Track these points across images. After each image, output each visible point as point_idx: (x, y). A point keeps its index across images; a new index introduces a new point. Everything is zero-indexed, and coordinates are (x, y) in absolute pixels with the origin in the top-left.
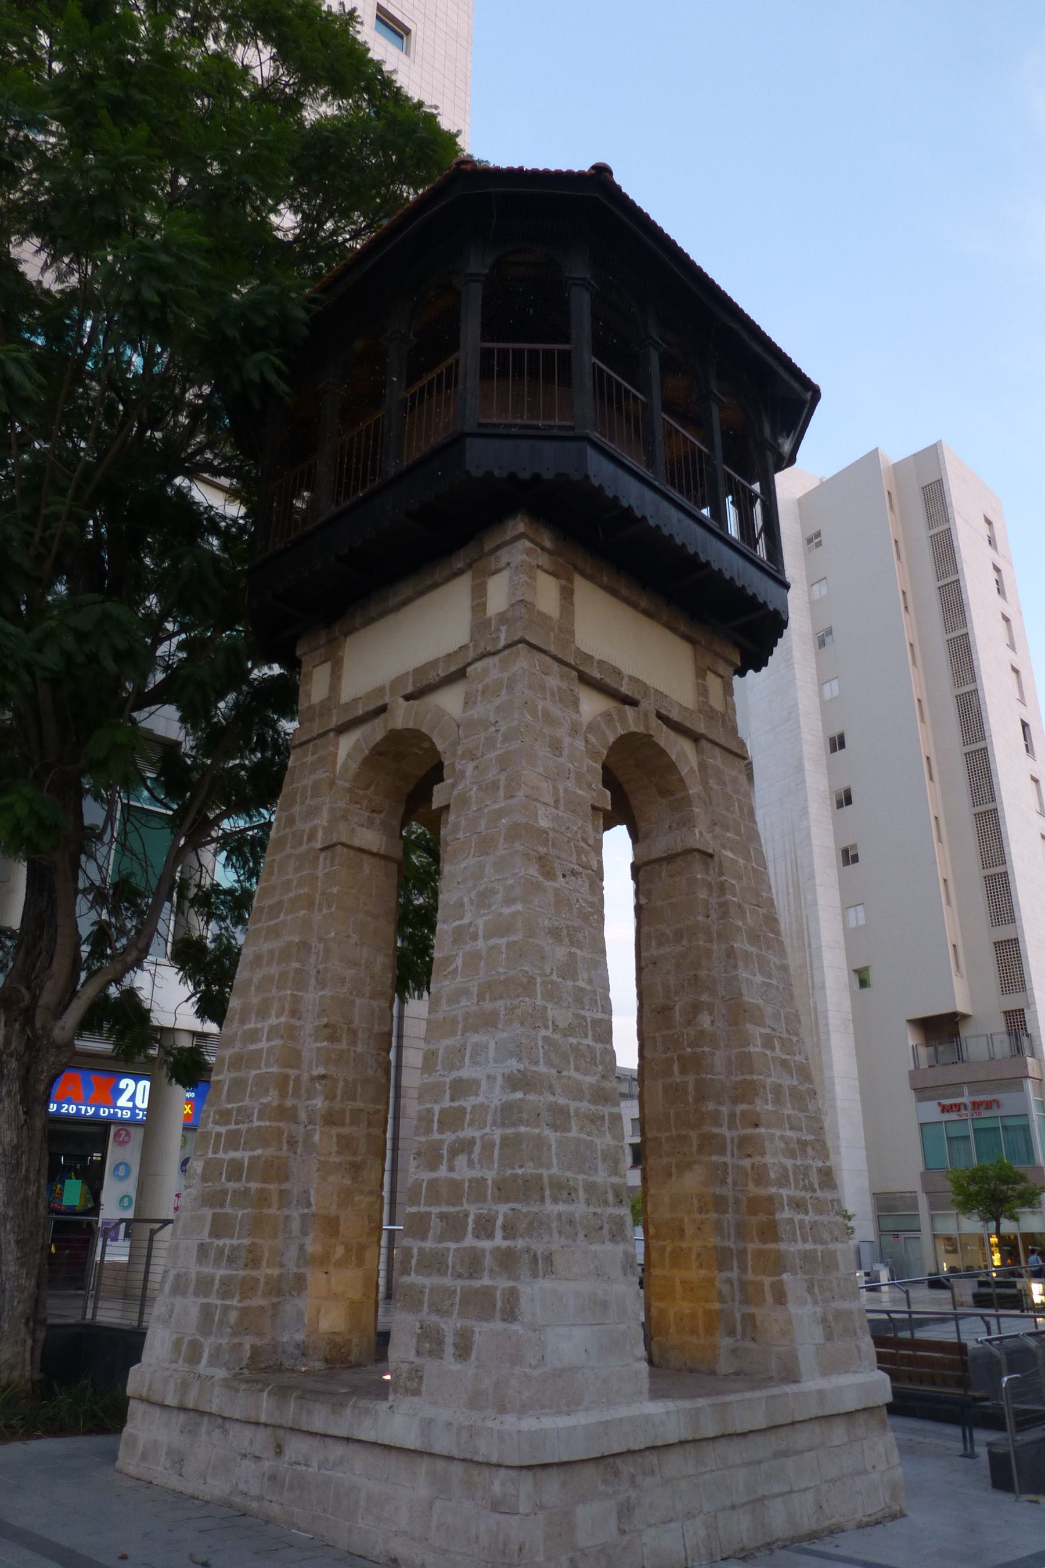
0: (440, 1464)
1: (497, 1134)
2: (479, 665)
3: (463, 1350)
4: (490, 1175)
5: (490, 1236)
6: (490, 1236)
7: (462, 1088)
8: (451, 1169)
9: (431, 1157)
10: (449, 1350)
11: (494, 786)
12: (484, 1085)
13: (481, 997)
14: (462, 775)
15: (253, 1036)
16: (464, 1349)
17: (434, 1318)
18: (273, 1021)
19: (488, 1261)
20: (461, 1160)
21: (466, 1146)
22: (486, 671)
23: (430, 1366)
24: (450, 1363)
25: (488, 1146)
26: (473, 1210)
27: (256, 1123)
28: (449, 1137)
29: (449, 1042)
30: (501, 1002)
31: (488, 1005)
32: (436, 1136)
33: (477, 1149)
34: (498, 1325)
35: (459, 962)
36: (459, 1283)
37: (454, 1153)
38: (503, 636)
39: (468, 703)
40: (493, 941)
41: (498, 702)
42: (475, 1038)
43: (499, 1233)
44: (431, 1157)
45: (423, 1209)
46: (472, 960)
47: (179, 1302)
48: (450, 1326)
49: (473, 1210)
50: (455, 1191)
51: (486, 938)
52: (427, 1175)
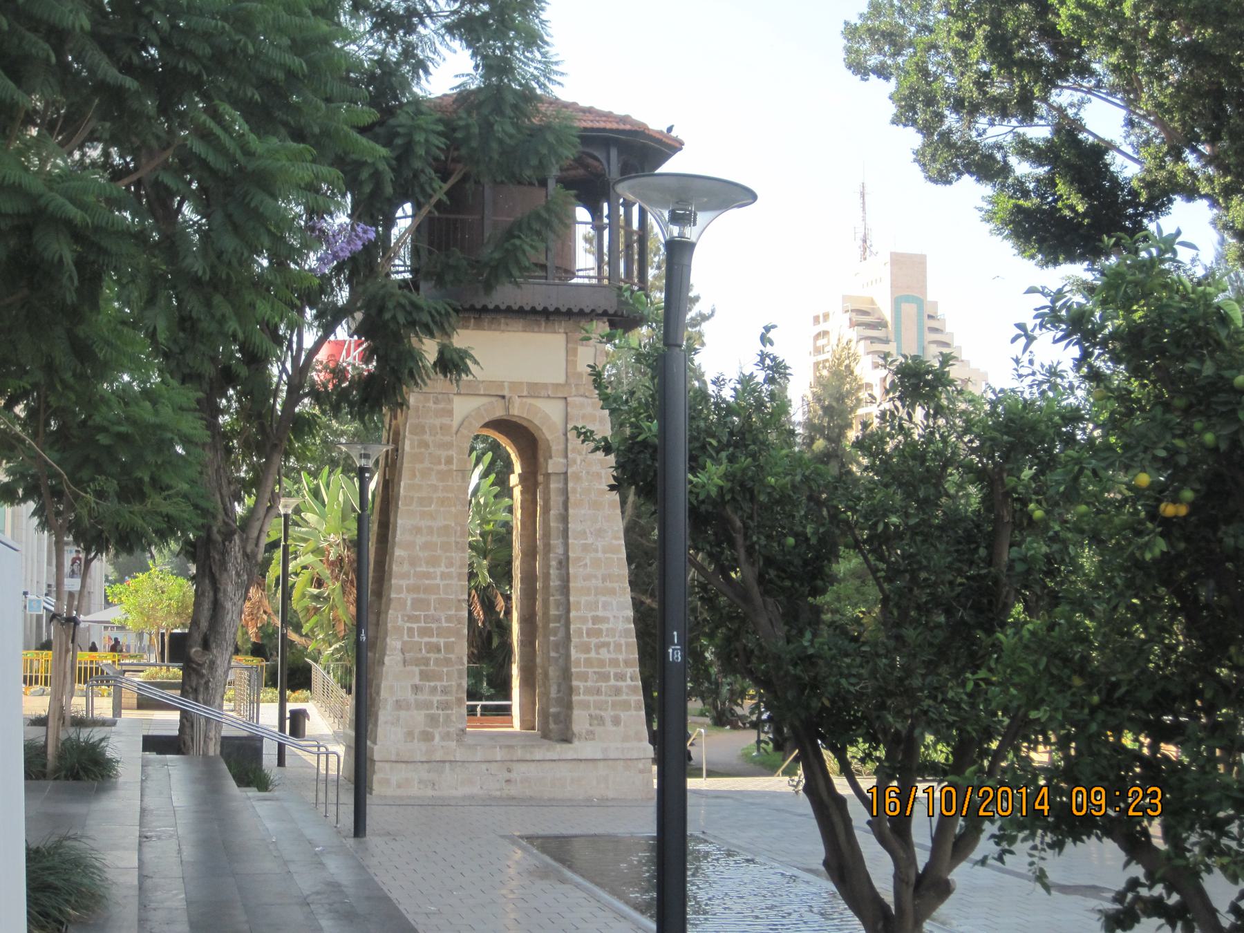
0: (610, 763)
1: (623, 641)
3: (616, 721)
4: (621, 657)
9: (586, 649)
15: (427, 575)
16: (616, 721)
17: (598, 712)
18: (443, 569)
19: (624, 689)
20: (603, 651)
21: (607, 645)
23: (598, 730)
24: (610, 727)
26: (613, 671)
27: (445, 625)
28: (594, 640)
34: (634, 713)
35: (588, 561)
36: (610, 699)
40: (608, 555)
42: (602, 599)
44: (586, 649)
45: (583, 669)
47: (403, 714)
48: (608, 714)
49: (613, 671)
50: (602, 663)
51: (604, 552)
52: (583, 656)
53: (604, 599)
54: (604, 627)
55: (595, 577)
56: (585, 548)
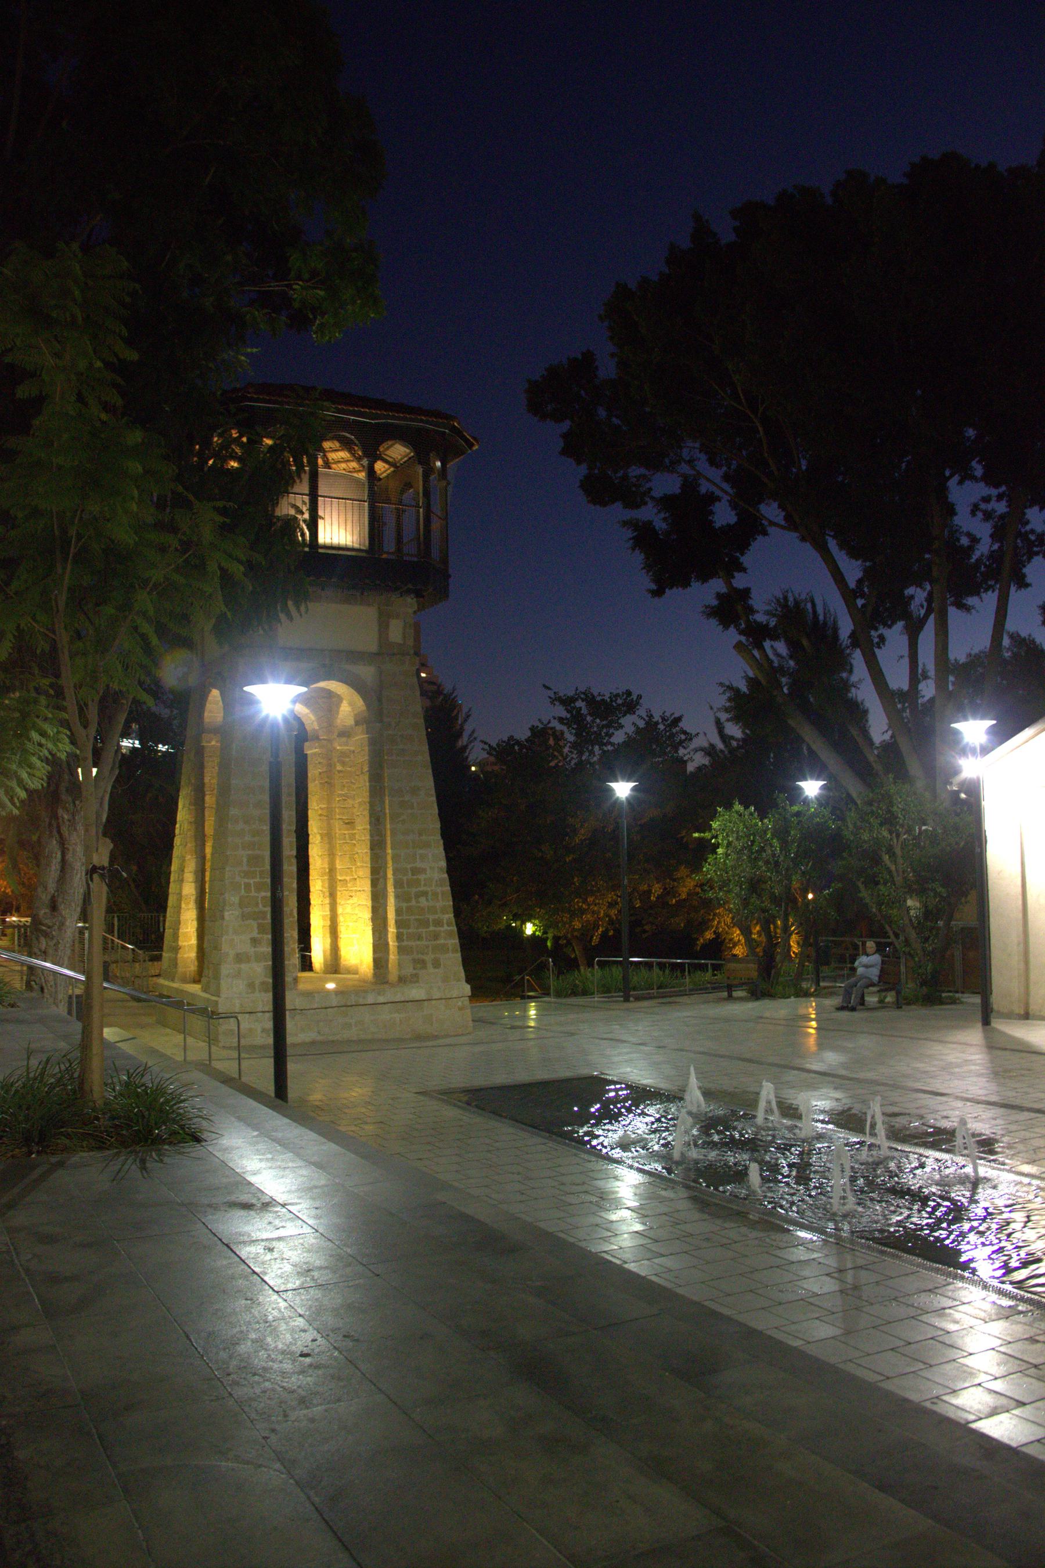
5: (442, 926)
6: (442, 926)
8: (418, 902)
10: (429, 965)
16: (436, 964)
20: (423, 900)
21: (425, 894)
24: (431, 969)
25: (435, 894)
28: (414, 890)
37: (418, 896)
48: (428, 958)
53: (421, 851)
54: (422, 877)
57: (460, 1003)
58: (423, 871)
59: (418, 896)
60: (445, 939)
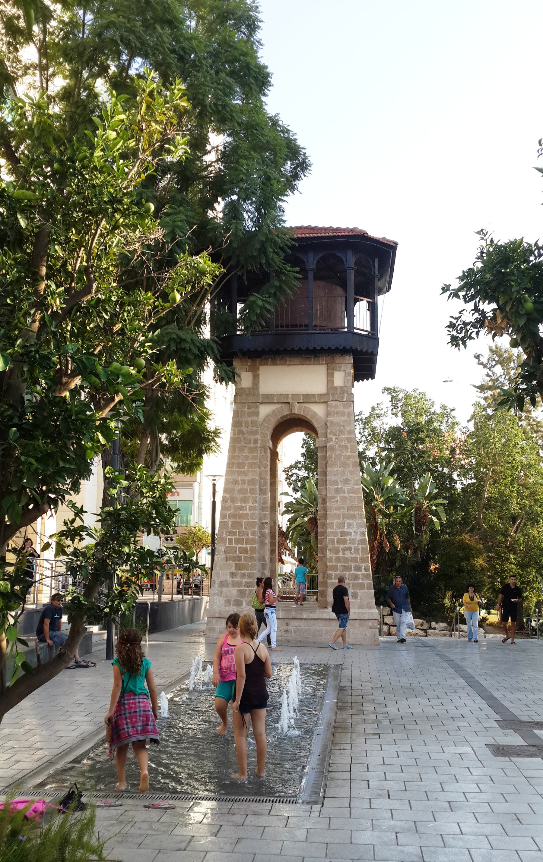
1: (360, 547)
2: (334, 403)
4: (358, 557)
5: (361, 571)
6: (361, 571)
7: (343, 534)
8: (344, 554)
11: (346, 447)
12: (353, 533)
13: (348, 510)
14: (331, 439)
19: (360, 576)
21: (350, 549)
22: (336, 406)
25: (357, 550)
26: (353, 565)
28: (342, 546)
29: (338, 521)
30: (356, 512)
31: (351, 512)
32: (336, 545)
33: (353, 550)
35: (338, 498)
36: (351, 582)
37: (344, 550)
38: (345, 397)
39: (328, 414)
41: (344, 419)
43: (363, 570)
44: (337, 551)
45: (334, 564)
46: (344, 499)
49: (353, 565)
50: (346, 560)
52: (334, 556)
53: (348, 521)
54: (348, 538)
55: (343, 508)
56: (337, 491)
57: (370, 624)
58: (349, 534)
59: (344, 550)
60: (362, 579)
